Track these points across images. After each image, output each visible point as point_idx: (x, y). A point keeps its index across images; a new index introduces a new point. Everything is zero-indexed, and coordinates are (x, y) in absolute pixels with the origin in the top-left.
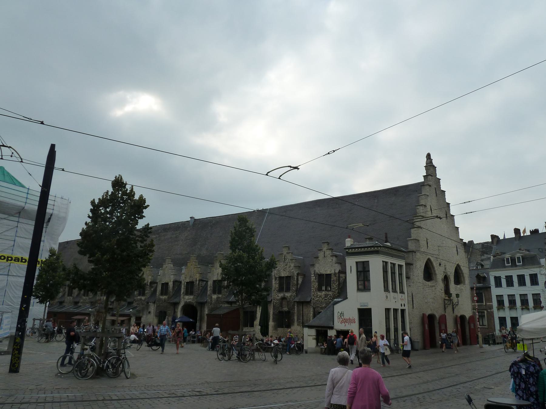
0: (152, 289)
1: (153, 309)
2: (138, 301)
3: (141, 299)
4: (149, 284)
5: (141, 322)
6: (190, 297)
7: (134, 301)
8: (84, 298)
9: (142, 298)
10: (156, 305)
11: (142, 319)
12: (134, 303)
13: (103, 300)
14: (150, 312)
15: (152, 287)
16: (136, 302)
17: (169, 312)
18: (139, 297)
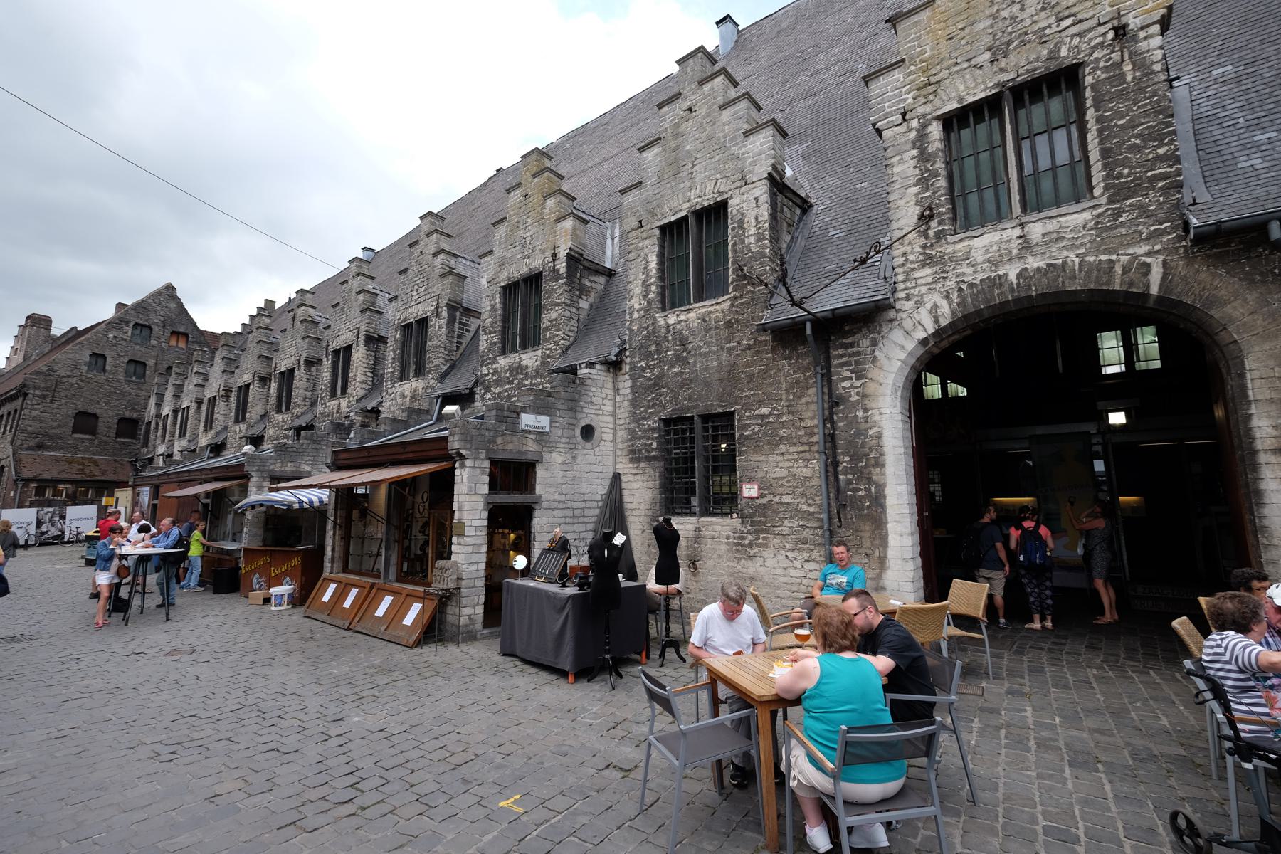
0: (584, 304)
1: (608, 408)
2: (498, 383)
3: (517, 369)
4: (562, 267)
5: (538, 501)
6: (1037, 230)
7: (478, 390)
8: (279, 418)
9: (524, 363)
10: (626, 384)
11: (540, 473)
12: (478, 397)
13: (338, 412)
14: (588, 432)
15: (583, 291)
16: (487, 390)
17: (765, 411)
18: (503, 362)
